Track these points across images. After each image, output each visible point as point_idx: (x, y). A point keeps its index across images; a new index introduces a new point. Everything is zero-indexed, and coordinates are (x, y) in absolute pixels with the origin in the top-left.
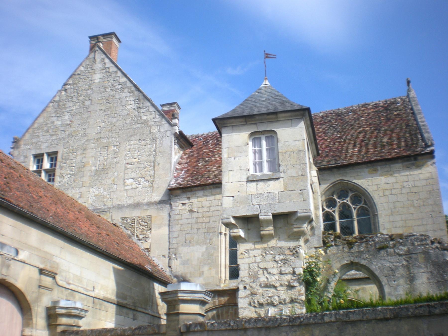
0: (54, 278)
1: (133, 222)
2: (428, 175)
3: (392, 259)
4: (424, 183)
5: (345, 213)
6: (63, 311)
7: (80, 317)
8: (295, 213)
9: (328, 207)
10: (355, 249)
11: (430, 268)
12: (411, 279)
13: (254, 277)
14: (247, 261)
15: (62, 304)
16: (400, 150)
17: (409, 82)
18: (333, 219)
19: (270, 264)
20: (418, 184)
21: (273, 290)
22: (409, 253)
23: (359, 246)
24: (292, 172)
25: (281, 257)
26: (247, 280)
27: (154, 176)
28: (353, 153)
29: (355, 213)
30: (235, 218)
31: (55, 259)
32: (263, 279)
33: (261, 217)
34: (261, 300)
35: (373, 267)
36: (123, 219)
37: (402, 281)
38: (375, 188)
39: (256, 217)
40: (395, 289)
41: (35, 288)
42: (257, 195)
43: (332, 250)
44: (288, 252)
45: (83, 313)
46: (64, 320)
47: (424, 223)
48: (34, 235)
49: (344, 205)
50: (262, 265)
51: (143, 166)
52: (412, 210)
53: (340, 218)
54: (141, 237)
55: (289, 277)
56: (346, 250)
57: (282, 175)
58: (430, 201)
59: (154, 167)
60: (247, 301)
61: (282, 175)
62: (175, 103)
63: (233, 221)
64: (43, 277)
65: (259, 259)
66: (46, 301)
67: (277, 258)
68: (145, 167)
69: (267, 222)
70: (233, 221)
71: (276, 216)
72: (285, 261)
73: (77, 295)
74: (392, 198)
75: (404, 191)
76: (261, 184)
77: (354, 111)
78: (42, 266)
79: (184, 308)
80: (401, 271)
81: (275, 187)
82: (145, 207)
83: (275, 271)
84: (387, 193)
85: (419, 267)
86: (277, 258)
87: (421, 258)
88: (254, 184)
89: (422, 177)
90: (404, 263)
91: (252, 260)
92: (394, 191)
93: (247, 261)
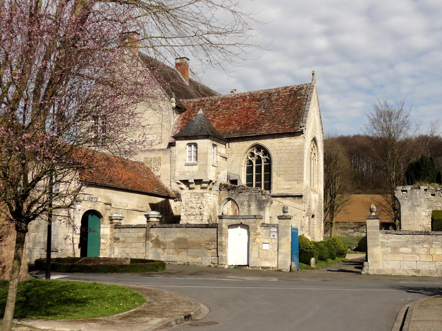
0: (111, 205)
1: (151, 161)
2: (299, 144)
3: (244, 197)
4: (297, 148)
5: (259, 161)
6: (115, 218)
7: (121, 220)
8: (202, 180)
9: (251, 157)
10: (230, 192)
11: (256, 202)
12: (249, 206)
13: (187, 204)
14: (185, 197)
15: (114, 215)
16: (289, 127)
17: (313, 74)
18: (252, 164)
19: (193, 199)
20: (294, 148)
21: (193, 209)
22: (249, 195)
23: (232, 191)
24: (202, 163)
25: (198, 196)
26: (184, 205)
27: (161, 133)
28: (265, 128)
29: (263, 161)
30: (180, 181)
31: (110, 198)
32: (190, 205)
33: (189, 181)
34: (189, 213)
35: (236, 200)
36: (145, 158)
37: (246, 207)
38: (273, 149)
39: (188, 180)
40: (243, 210)
41: (104, 210)
42: (188, 172)
43: (222, 192)
44: (200, 195)
45: (122, 218)
46: (115, 221)
47: (294, 169)
48: (102, 191)
49: (259, 157)
50: (190, 200)
51: (155, 127)
52: (289, 162)
53: (256, 163)
54: (155, 169)
55: (200, 205)
56: (227, 192)
57: (198, 163)
58: (298, 158)
59: (162, 128)
60: (184, 213)
61: (198, 163)
62: (184, 58)
63: (179, 182)
64: (107, 206)
65: (189, 197)
66: (108, 214)
67: (196, 197)
68: (157, 128)
69: (192, 183)
70: (179, 182)
71: (195, 180)
72: (199, 198)
73: (120, 210)
74: (281, 155)
75: (287, 151)
76: (190, 166)
77: (279, 93)
78: (106, 202)
79: (151, 219)
80: (246, 203)
81: (195, 168)
82: (157, 152)
83: (194, 202)
84: (278, 152)
85: (252, 201)
86: (196, 197)
87: (254, 198)
88: (187, 166)
89: (296, 144)
90: (248, 199)
91: (187, 197)
92: (282, 151)
93: (185, 197)
